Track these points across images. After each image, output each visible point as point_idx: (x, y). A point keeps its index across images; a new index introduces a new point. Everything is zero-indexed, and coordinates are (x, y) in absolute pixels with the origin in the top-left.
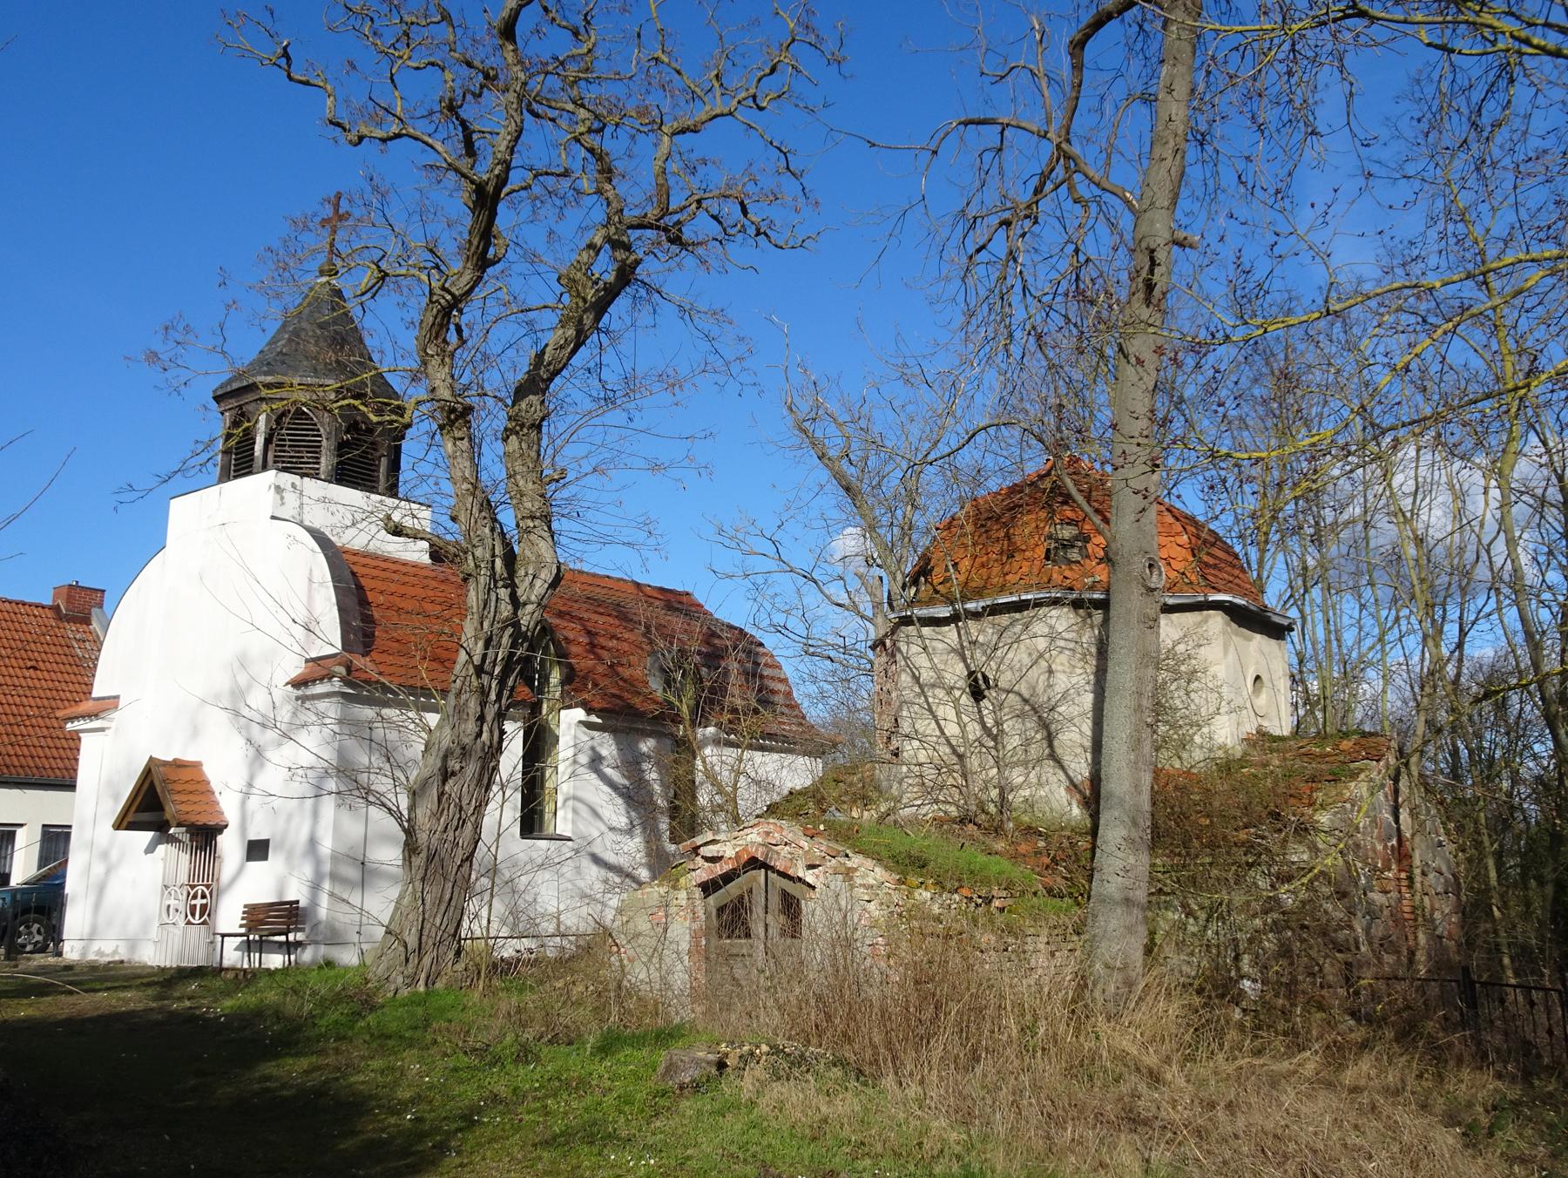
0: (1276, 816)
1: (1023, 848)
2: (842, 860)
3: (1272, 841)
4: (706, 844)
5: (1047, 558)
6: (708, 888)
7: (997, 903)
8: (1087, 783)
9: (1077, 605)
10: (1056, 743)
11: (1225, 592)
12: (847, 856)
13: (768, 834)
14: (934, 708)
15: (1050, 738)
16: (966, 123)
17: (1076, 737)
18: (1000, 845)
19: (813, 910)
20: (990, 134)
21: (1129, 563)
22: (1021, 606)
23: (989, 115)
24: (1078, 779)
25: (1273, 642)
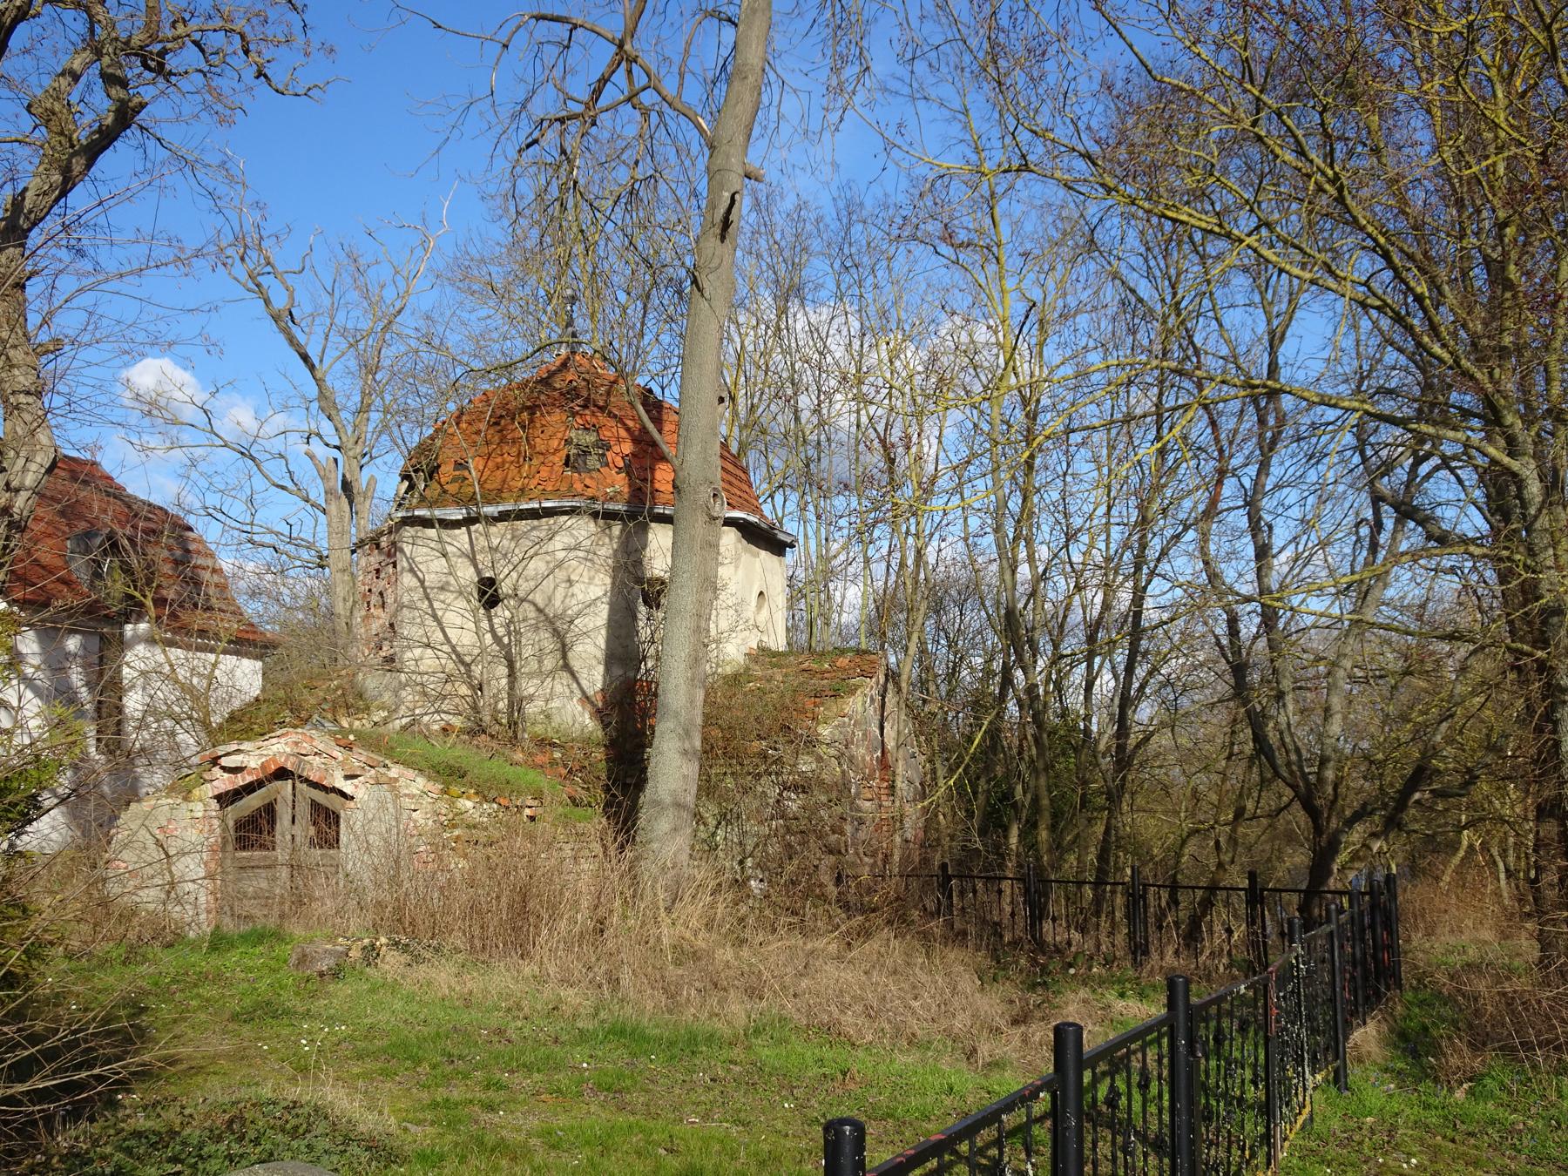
0: (786, 728)
1: (540, 759)
2: (383, 770)
3: (785, 751)
4: (228, 754)
5: (567, 464)
6: (225, 799)
7: (528, 812)
8: (599, 697)
9: (595, 515)
10: (570, 655)
11: (741, 508)
12: (385, 766)
13: (296, 744)
14: (440, 613)
15: (564, 650)
16: (539, 18)
17: (591, 649)
18: (519, 756)
19: (353, 820)
20: (561, 30)
21: (696, 493)
22: (534, 514)
23: (564, 13)
24: (590, 692)
25: (775, 558)
